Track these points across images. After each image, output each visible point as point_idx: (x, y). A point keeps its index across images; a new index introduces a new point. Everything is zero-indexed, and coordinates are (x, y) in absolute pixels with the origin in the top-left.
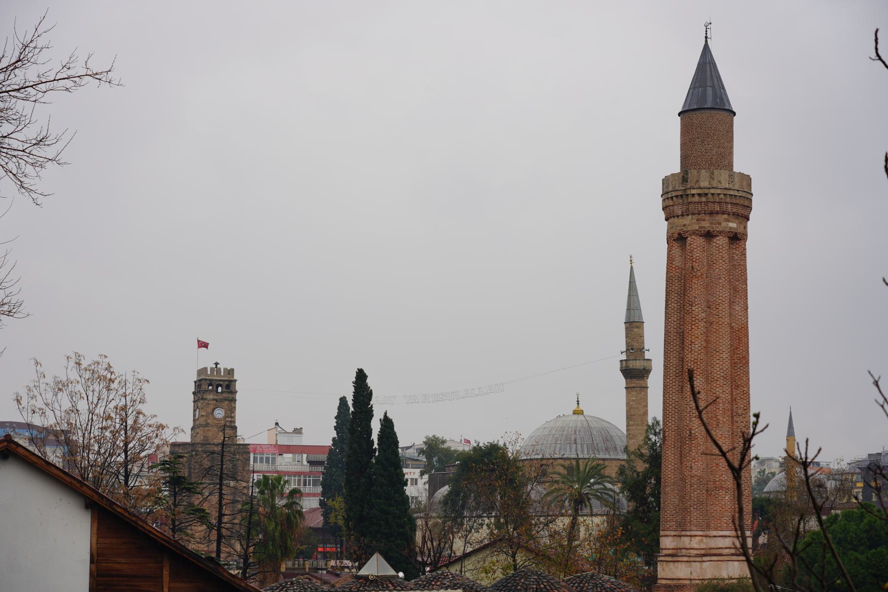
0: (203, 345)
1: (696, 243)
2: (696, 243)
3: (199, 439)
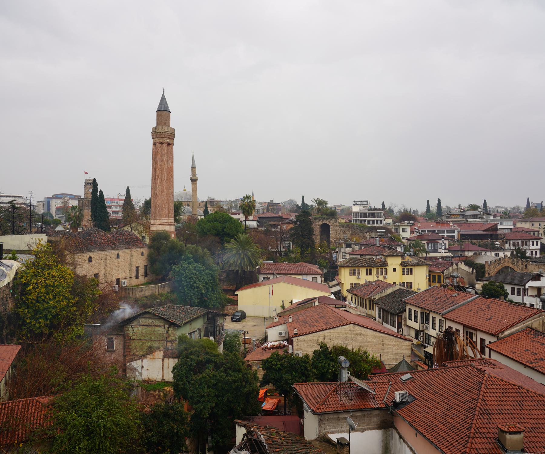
0: (86, 173)
1: (158, 145)
2: (158, 145)
3: (86, 197)
